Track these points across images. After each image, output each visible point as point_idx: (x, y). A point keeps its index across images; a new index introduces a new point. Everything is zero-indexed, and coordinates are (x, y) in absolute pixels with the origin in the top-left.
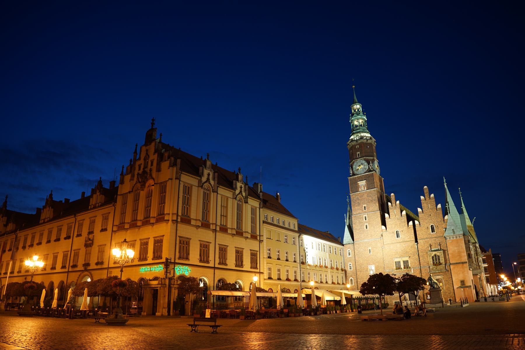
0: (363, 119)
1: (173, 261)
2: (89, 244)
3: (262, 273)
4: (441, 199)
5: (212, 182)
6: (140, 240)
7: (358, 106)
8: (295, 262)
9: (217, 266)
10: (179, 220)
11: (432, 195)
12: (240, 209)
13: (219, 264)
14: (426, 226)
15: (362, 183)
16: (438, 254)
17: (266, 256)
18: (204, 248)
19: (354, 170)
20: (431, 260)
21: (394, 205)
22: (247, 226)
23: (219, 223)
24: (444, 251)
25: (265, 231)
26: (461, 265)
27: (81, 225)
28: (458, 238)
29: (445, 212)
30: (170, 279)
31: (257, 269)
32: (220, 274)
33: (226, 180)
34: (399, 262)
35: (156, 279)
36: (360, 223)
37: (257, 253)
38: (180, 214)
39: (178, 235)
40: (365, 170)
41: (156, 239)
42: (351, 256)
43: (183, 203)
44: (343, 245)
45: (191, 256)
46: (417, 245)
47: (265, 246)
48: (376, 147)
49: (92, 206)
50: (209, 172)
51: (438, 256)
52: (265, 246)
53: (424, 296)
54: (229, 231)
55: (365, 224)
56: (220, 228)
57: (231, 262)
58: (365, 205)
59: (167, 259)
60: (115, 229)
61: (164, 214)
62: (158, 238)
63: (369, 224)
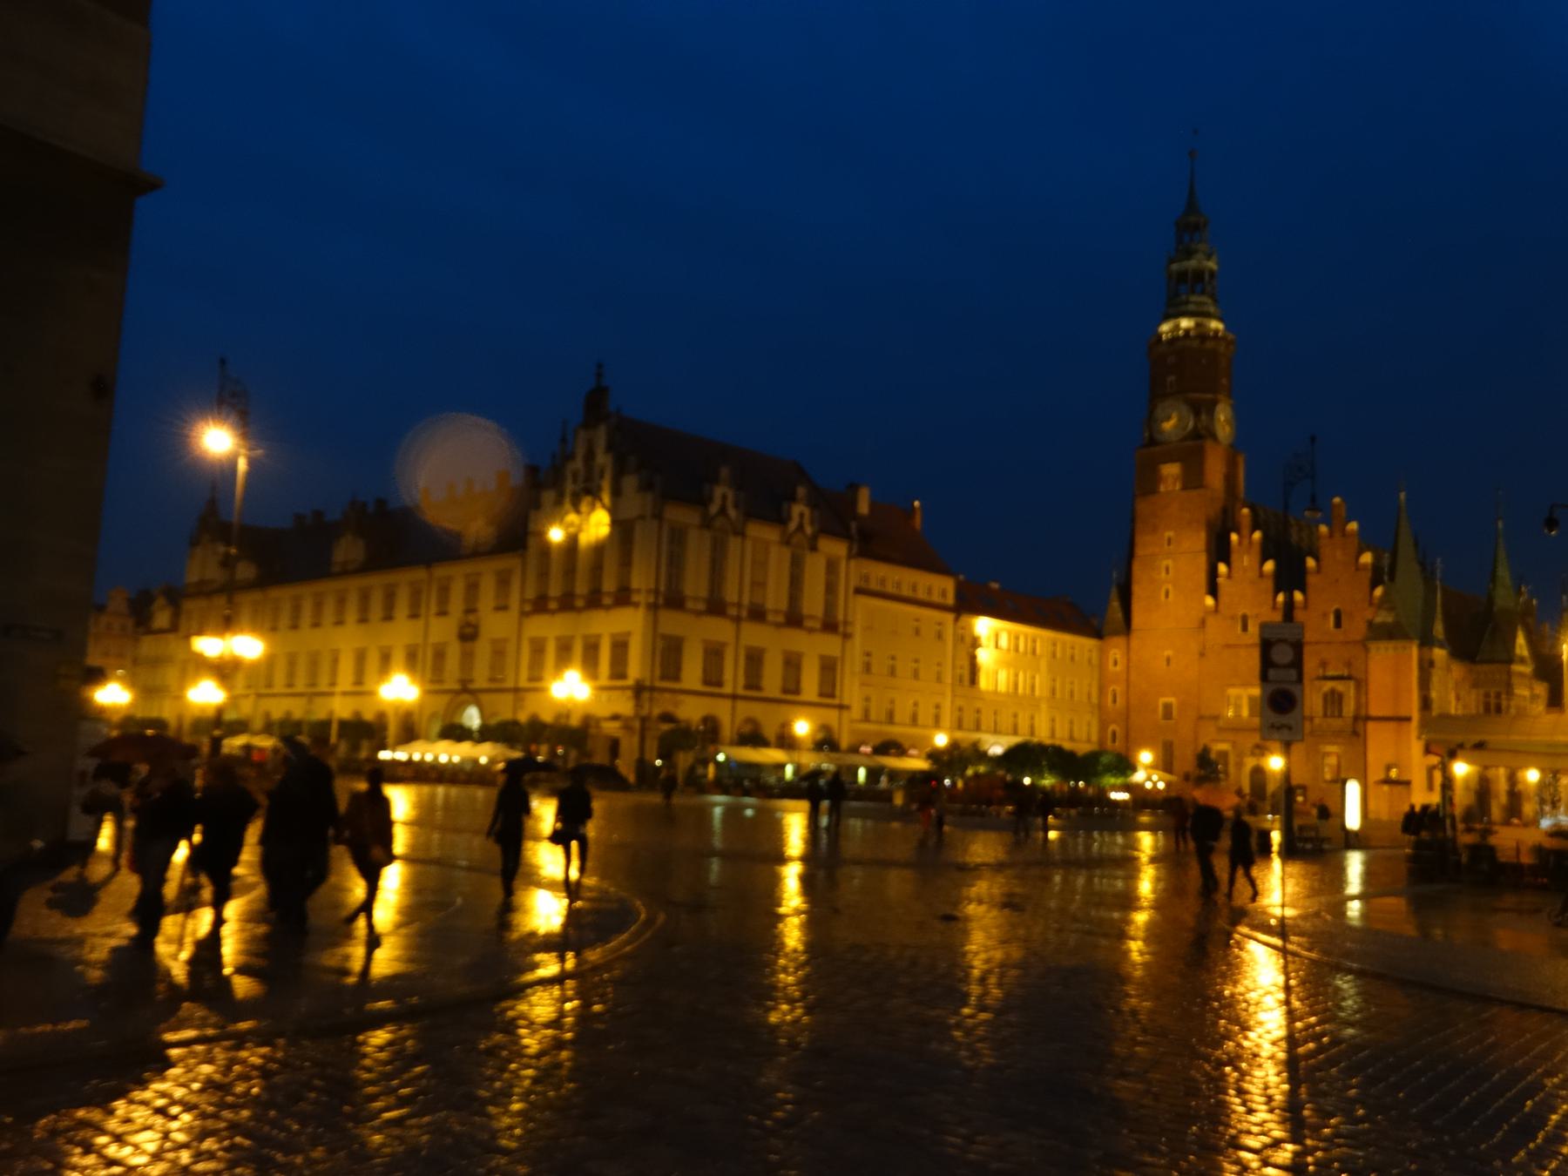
1: (648, 683)
2: (468, 634)
5: (732, 513)
8: (939, 679)
9: (741, 691)
10: (661, 601)
11: (1353, 526)
12: (797, 566)
15: (1171, 470)
17: (858, 667)
18: (714, 654)
21: (1246, 542)
22: (813, 603)
26: (1392, 725)
27: (444, 592)
30: (644, 720)
31: (832, 696)
32: (745, 709)
33: (766, 502)
35: (615, 717)
42: (1118, 668)
54: (770, 617)
57: (772, 681)
60: (528, 608)
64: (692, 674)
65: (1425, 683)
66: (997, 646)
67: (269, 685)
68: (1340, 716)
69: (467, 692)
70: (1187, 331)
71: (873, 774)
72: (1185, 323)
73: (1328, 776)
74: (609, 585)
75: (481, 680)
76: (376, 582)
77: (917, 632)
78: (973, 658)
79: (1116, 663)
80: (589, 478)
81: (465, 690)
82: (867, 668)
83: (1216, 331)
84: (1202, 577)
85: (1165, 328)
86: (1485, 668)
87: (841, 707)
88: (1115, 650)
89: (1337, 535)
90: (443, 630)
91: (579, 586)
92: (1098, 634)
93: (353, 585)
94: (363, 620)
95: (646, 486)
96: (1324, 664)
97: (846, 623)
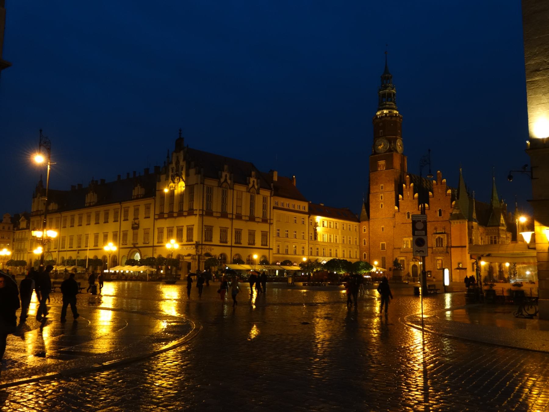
1: (200, 243)
2: (135, 227)
3: (272, 249)
5: (229, 181)
9: (233, 245)
10: (204, 213)
11: (444, 180)
12: (252, 199)
13: (236, 243)
16: (442, 237)
18: (224, 231)
21: (408, 187)
22: (258, 213)
23: (235, 213)
26: (460, 249)
27: (126, 212)
30: (199, 256)
31: (267, 245)
32: (235, 251)
33: (241, 177)
35: (189, 255)
38: (205, 209)
39: (204, 224)
40: (385, 150)
43: (207, 200)
45: (213, 239)
47: (275, 227)
51: (442, 239)
56: (236, 216)
57: (245, 241)
58: (383, 185)
60: (157, 217)
61: (193, 209)
64: (216, 239)
65: (470, 234)
66: (323, 226)
67: (63, 248)
68: (442, 246)
69: (135, 248)
70: (386, 114)
71: (281, 272)
72: (385, 111)
73: (438, 268)
74: (186, 208)
75: (140, 244)
76: (102, 209)
77: (295, 222)
78: (316, 230)
80: (177, 171)
81: (135, 247)
82: (278, 235)
83: (396, 114)
84: (394, 199)
85: (378, 113)
86: (491, 228)
87: (269, 249)
88: (364, 226)
89: (439, 183)
90: (126, 226)
91: (175, 209)
92: (359, 221)
93: (93, 210)
94: (97, 223)
95: (198, 173)
96: (436, 229)
97: (270, 219)
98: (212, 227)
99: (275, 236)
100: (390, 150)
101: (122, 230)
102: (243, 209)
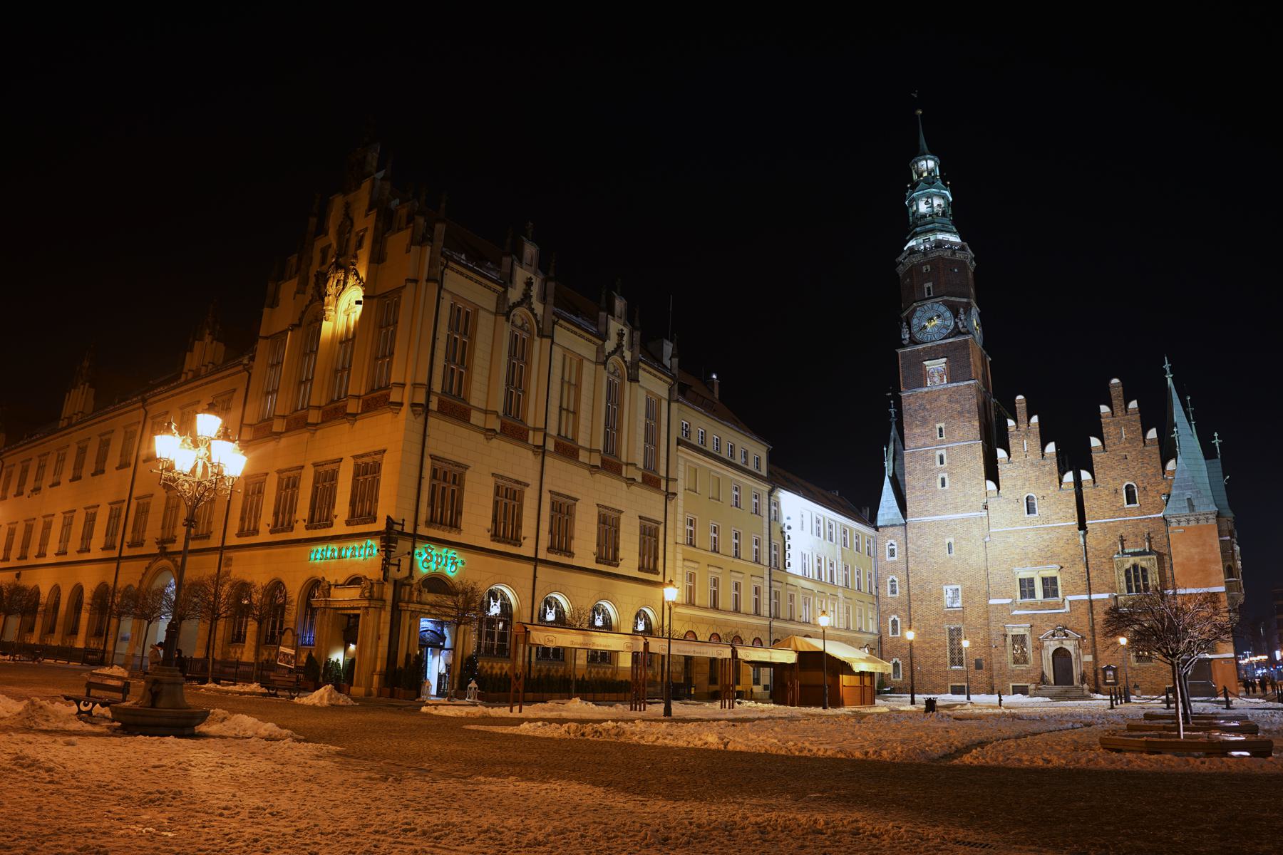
0: (944, 197)
1: (408, 529)
4: (1155, 415)
5: (538, 308)
6: (315, 465)
7: (931, 164)
8: (757, 561)
9: (543, 555)
10: (434, 405)
11: (1133, 404)
13: (551, 549)
14: (1113, 485)
16: (1144, 564)
19: (915, 330)
20: (1123, 578)
21: (1023, 426)
22: (633, 449)
23: (552, 430)
24: (1161, 557)
25: (681, 468)
28: (1202, 523)
29: (1168, 450)
30: (398, 585)
31: (658, 573)
34: (1031, 581)
35: (355, 581)
36: (925, 471)
37: (657, 529)
38: (437, 387)
39: (427, 451)
41: (359, 461)
42: (895, 558)
43: (450, 358)
44: (877, 529)
45: (465, 519)
46: (1084, 537)
47: (680, 510)
48: (975, 273)
49: (190, 375)
50: (529, 275)
51: (1144, 570)
52: (680, 510)
53: (1096, 674)
54: (583, 456)
55: (940, 476)
56: (557, 445)
58: (943, 425)
59: (390, 521)
62: (366, 460)
63: (951, 474)
74: (358, 385)
79: (892, 553)
80: (342, 252)
81: (164, 553)
98: (466, 467)
99: (680, 540)
100: (956, 332)
101: (135, 494)
102: (582, 421)
